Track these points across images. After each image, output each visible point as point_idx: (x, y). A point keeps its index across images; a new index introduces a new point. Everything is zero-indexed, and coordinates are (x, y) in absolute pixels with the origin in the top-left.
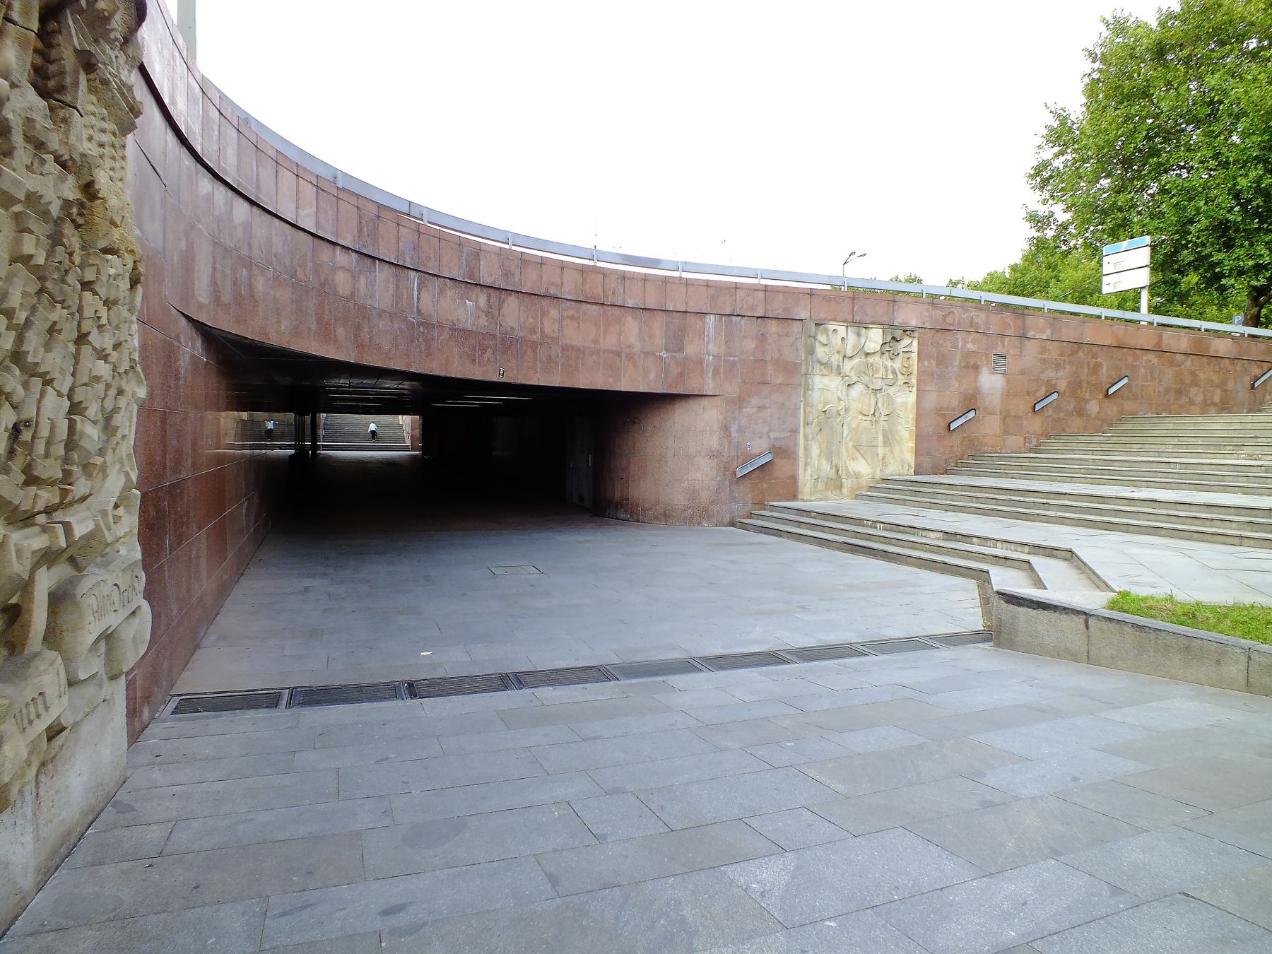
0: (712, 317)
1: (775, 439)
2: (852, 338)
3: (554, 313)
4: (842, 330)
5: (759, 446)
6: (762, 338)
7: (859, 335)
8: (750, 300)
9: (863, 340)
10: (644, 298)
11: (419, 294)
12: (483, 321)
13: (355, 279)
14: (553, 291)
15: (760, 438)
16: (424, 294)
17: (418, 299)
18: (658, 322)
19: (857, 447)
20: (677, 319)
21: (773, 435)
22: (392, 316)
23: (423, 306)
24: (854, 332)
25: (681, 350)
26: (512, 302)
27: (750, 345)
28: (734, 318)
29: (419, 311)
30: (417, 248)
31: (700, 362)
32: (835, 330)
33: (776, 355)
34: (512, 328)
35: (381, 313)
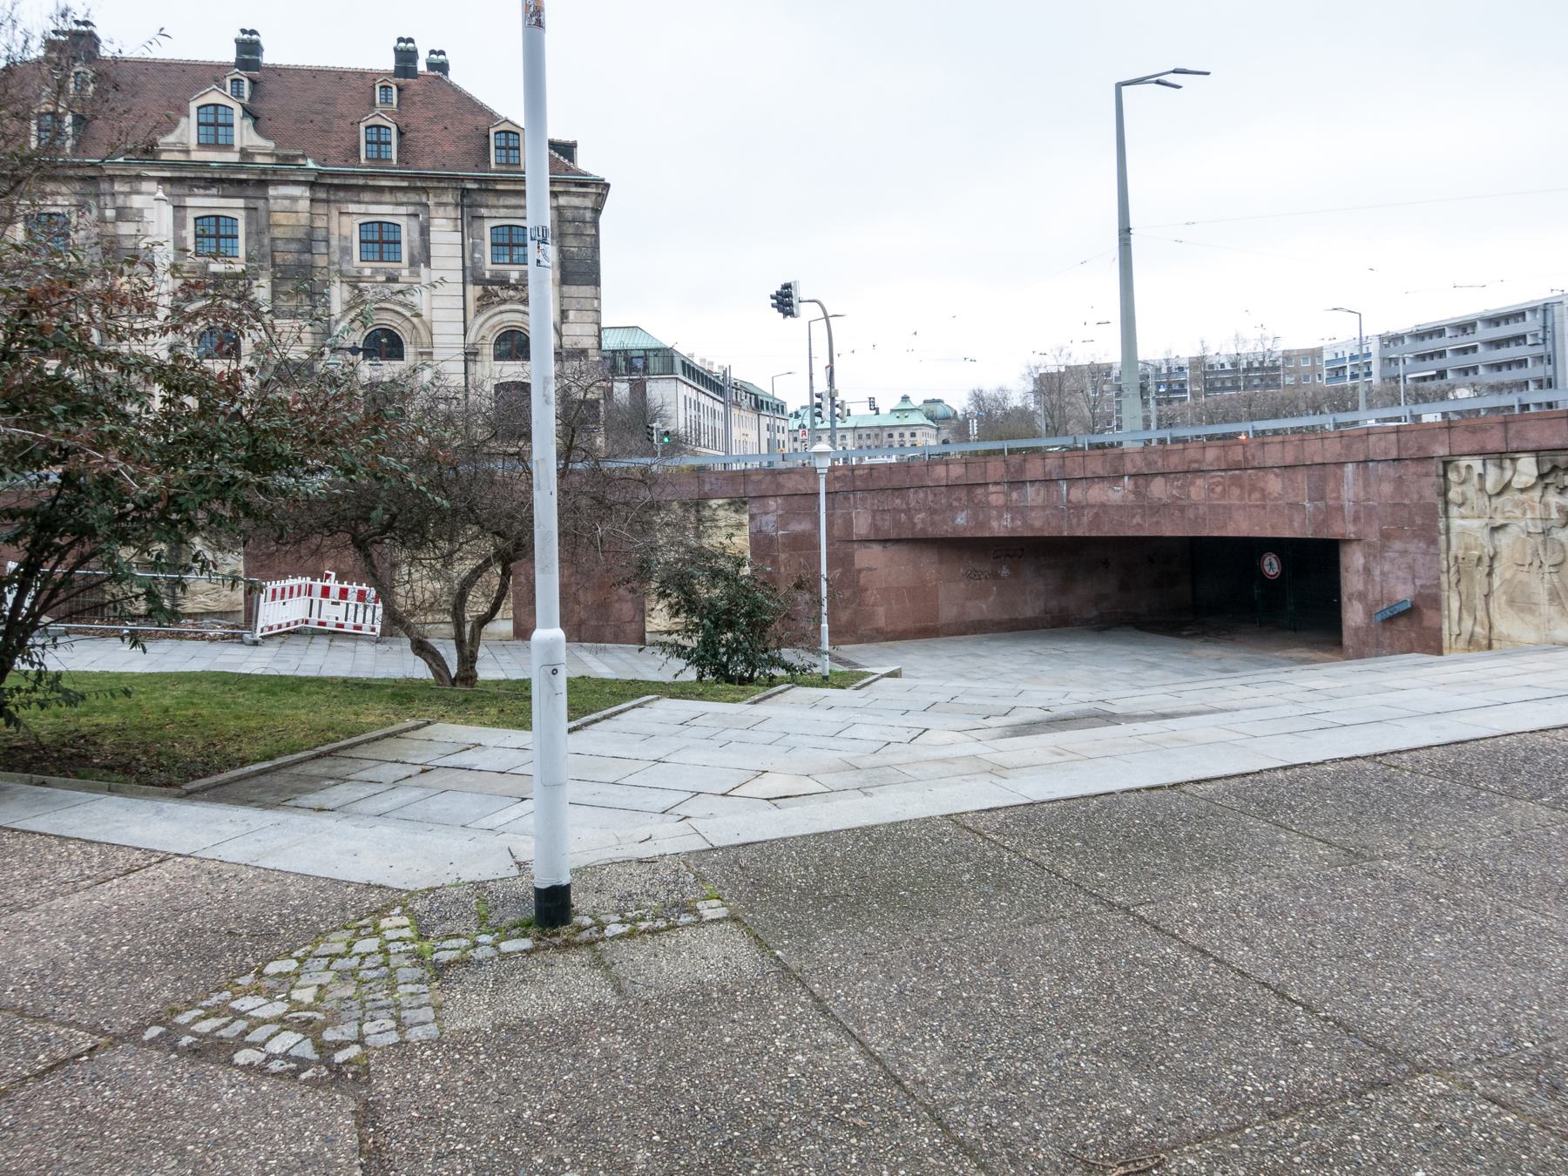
0: (1350, 465)
1: (1422, 586)
2: (1492, 472)
3: (1199, 482)
4: (1477, 464)
5: (1403, 592)
6: (1400, 481)
7: (1501, 468)
8: (1383, 444)
9: (1508, 474)
10: (1283, 457)
11: (1068, 490)
12: (1131, 497)
13: (1007, 495)
14: (1195, 466)
15: (1405, 583)
16: (1071, 491)
17: (1068, 494)
18: (1301, 477)
19: (1511, 602)
20: (1316, 472)
21: (1418, 582)
22: (1043, 508)
23: (1072, 497)
24: (1495, 465)
25: (1322, 498)
26: (1159, 481)
27: (1387, 488)
28: (1371, 464)
29: (1069, 501)
30: (1062, 467)
31: (1341, 508)
32: (1469, 467)
34: (1160, 499)
35: (1032, 508)
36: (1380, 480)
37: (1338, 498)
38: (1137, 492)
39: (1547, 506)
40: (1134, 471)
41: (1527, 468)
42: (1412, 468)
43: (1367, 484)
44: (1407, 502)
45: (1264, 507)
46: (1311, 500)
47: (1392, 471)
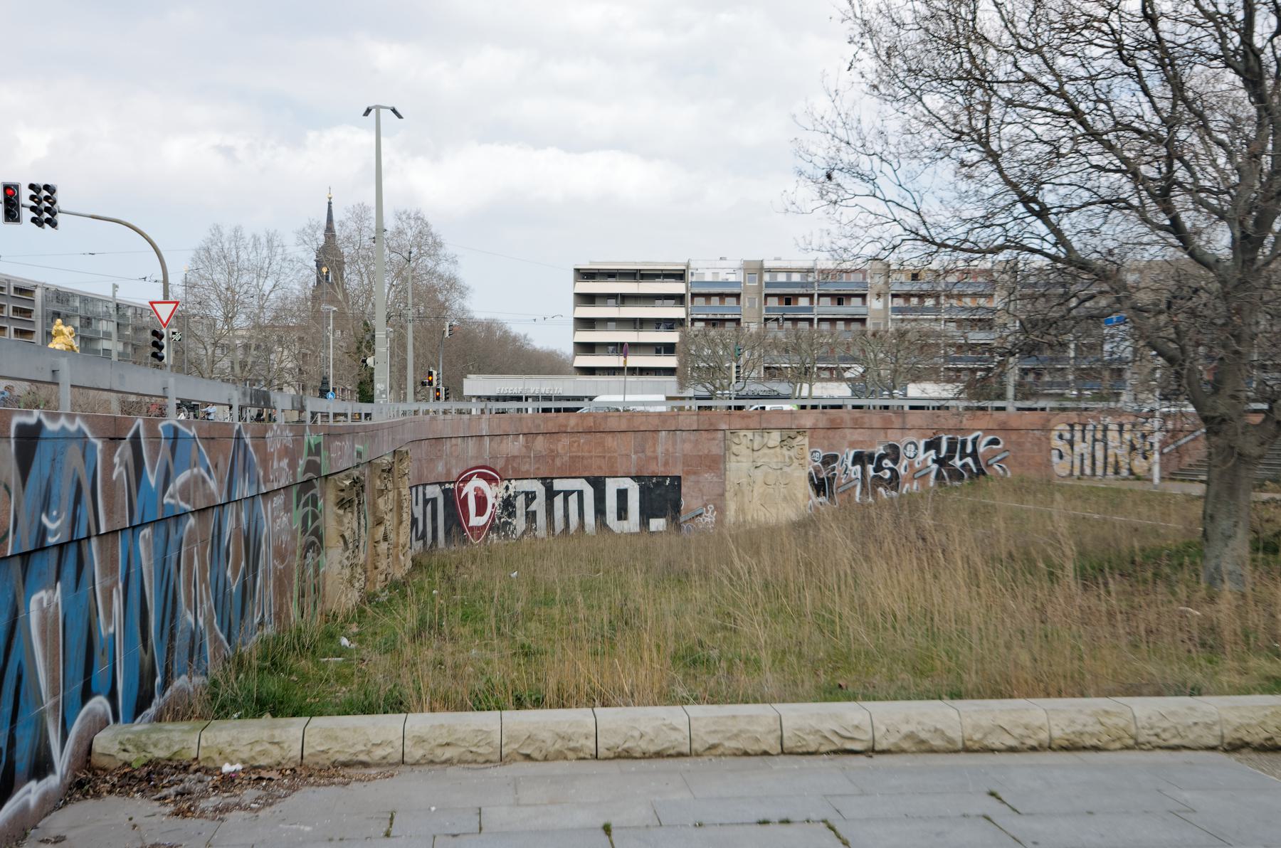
4: (750, 434)
12: (524, 450)
21: (705, 498)
25: (643, 451)
26: (540, 438)
31: (656, 458)
33: (706, 452)
36: (684, 441)
37: (654, 451)
38: (527, 447)
39: (784, 456)
40: (526, 431)
41: (775, 437)
42: (704, 434)
43: (674, 444)
44: (700, 453)
45: (604, 457)
46: (636, 453)
47: (692, 436)
